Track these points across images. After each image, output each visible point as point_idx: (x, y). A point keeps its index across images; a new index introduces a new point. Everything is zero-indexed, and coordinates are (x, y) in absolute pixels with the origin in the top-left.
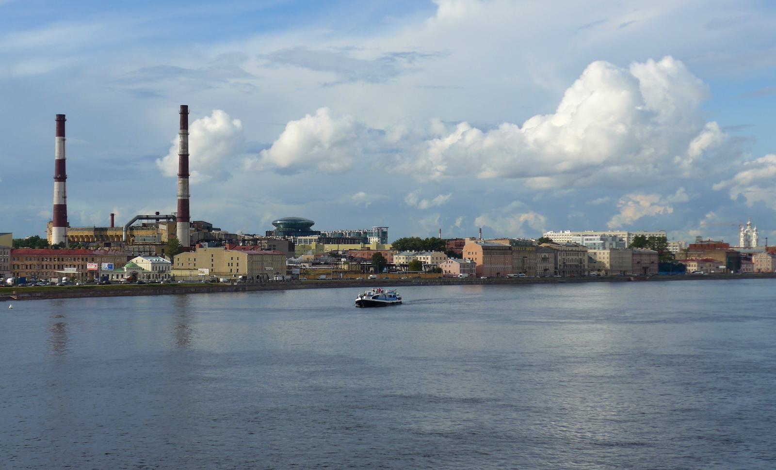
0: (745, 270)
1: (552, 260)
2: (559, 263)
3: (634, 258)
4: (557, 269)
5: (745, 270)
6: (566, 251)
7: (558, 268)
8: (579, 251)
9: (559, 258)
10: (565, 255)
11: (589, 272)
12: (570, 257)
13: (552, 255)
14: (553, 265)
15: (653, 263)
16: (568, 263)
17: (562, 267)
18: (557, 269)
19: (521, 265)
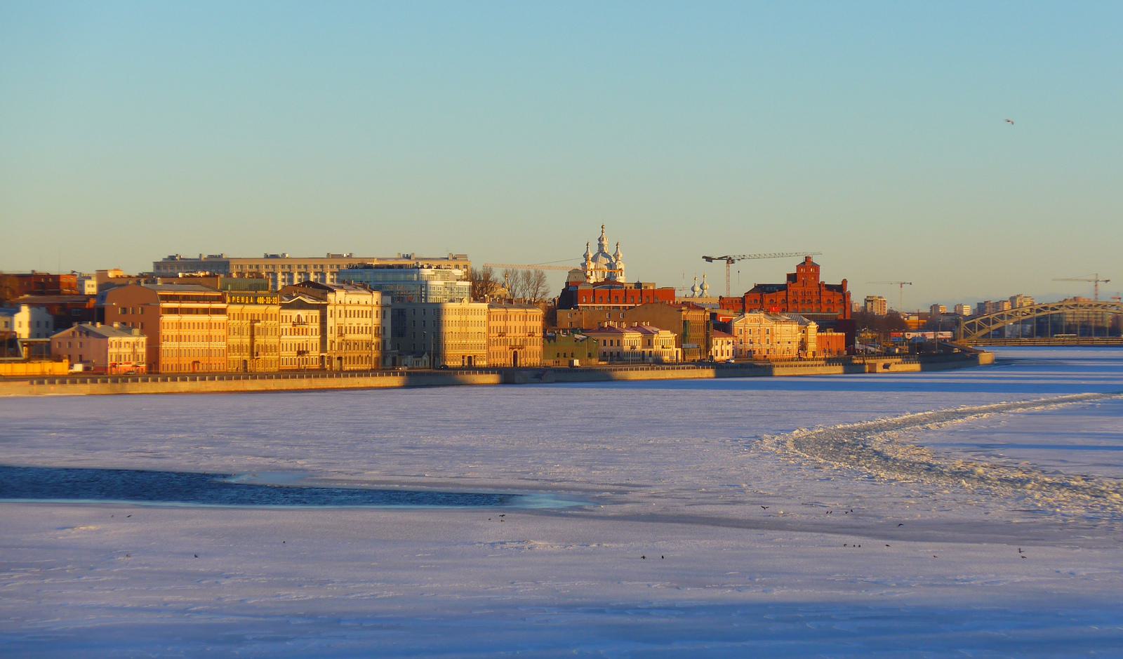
0: (719, 353)
1: (316, 326)
2: (329, 335)
3: (493, 324)
4: (326, 352)
5: (719, 353)
6: (345, 305)
7: (328, 348)
8: (372, 306)
9: (330, 322)
10: (343, 315)
11: (394, 359)
12: (354, 322)
13: (316, 313)
14: (316, 339)
15: (531, 334)
16: (349, 337)
17: (336, 347)
18: (326, 352)
19: (247, 341)
